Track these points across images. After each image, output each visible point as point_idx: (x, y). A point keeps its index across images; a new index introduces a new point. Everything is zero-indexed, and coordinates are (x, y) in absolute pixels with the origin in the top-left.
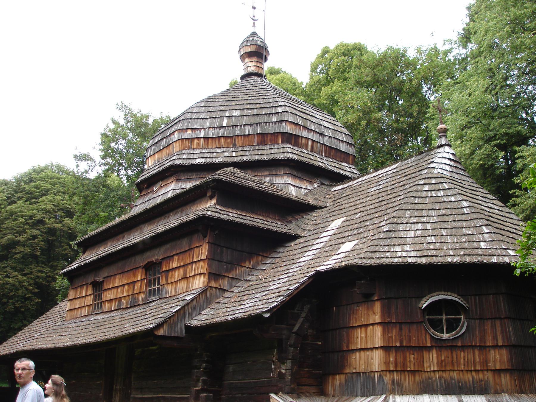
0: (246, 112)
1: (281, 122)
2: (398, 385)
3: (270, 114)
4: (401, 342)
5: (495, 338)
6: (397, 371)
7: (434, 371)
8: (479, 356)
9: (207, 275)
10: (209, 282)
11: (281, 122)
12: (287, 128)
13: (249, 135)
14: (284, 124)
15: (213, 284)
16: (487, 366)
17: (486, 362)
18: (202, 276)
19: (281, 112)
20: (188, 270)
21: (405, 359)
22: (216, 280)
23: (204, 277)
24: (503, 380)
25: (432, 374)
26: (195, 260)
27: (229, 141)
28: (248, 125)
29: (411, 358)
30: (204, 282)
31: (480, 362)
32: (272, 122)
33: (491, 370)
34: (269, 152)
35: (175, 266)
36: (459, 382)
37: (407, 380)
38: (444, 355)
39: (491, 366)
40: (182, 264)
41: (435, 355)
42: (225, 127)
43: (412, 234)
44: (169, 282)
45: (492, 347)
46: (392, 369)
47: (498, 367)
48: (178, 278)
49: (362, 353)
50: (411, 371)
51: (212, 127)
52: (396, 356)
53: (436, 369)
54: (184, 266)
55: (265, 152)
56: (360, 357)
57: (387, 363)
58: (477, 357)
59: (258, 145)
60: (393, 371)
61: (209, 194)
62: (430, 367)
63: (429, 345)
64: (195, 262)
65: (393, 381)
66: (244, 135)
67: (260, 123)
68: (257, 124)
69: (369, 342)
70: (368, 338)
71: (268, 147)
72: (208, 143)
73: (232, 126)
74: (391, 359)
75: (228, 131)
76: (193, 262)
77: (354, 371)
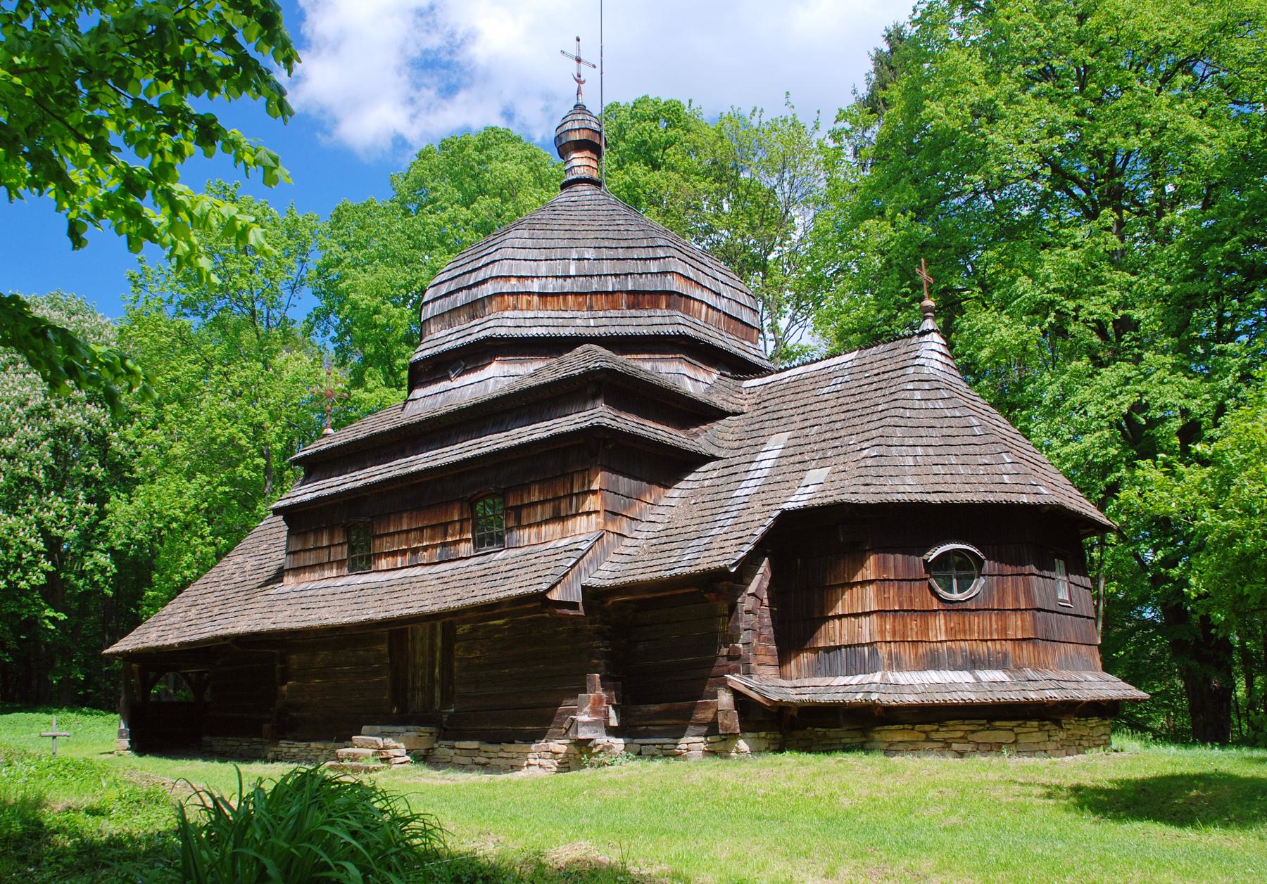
0: (605, 253)
1: (665, 273)
2: (896, 658)
3: (646, 259)
4: (900, 604)
5: (1017, 599)
6: (895, 642)
7: (941, 642)
8: (996, 622)
9: (602, 513)
10: (605, 524)
11: (665, 273)
12: (675, 285)
13: (613, 292)
14: (669, 277)
15: (610, 528)
16: (1006, 634)
17: (1004, 629)
18: (594, 515)
19: (664, 258)
20: (563, 505)
21: (905, 626)
22: (614, 521)
23: (597, 518)
24: (1025, 652)
25: (939, 644)
26: (575, 491)
27: (581, 299)
28: (611, 275)
29: (914, 625)
30: (597, 524)
31: (997, 629)
32: (651, 273)
33: (1011, 640)
34: (648, 321)
35: (534, 498)
36: (971, 653)
37: (907, 653)
38: (955, 619)
39: (1011, 634)
40: (550, 497)
41: (942, 621)
42: (574, 276)
43: (910, 461)
44: (525, 523)
45: (1013, 610)
46: (888, 639)
47: (1019, 637)
48: (542, 516)
49: (844, 620)
50: (913, 641)
51: (553, 277)
52: (894, 622)
53: (943, 638)
54: (553, 500)
55: (641, 321)
56: (841, 625)
57: (882, 632)
58: (994, 623)
59: (629, 308)
60: (890, 642)
61: (589, 391)
62: (936, 636)
63: (936, 608)
64: (577, 495)
65: (890, 654)
66: (607, 293)
67: (631, 274)
68: (626, 275)
69: (855, 606)
70: (855, 600)
71: (645, 313)
72: (546, 302)
73: (586, 276)
74: (888, 627)
75: (579, 284)
76: (571, 495)
77: (832, 644)
